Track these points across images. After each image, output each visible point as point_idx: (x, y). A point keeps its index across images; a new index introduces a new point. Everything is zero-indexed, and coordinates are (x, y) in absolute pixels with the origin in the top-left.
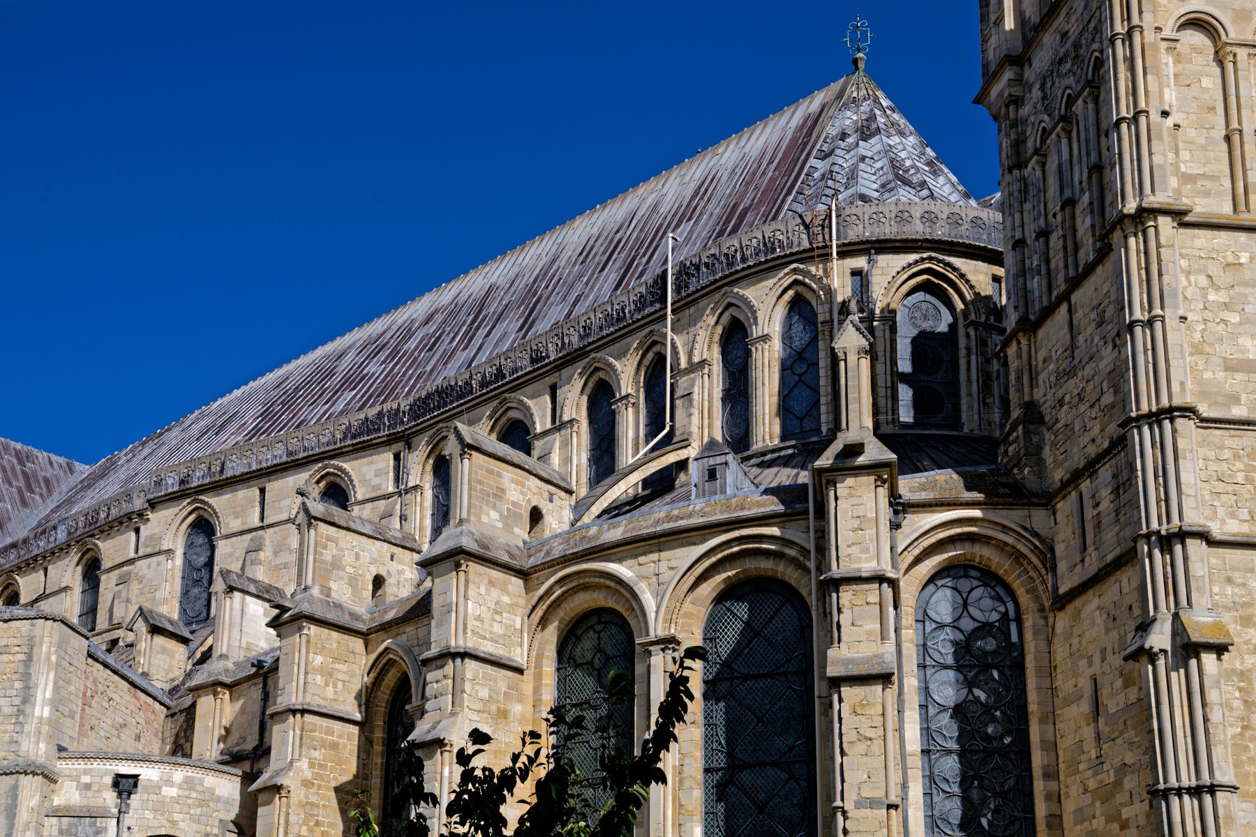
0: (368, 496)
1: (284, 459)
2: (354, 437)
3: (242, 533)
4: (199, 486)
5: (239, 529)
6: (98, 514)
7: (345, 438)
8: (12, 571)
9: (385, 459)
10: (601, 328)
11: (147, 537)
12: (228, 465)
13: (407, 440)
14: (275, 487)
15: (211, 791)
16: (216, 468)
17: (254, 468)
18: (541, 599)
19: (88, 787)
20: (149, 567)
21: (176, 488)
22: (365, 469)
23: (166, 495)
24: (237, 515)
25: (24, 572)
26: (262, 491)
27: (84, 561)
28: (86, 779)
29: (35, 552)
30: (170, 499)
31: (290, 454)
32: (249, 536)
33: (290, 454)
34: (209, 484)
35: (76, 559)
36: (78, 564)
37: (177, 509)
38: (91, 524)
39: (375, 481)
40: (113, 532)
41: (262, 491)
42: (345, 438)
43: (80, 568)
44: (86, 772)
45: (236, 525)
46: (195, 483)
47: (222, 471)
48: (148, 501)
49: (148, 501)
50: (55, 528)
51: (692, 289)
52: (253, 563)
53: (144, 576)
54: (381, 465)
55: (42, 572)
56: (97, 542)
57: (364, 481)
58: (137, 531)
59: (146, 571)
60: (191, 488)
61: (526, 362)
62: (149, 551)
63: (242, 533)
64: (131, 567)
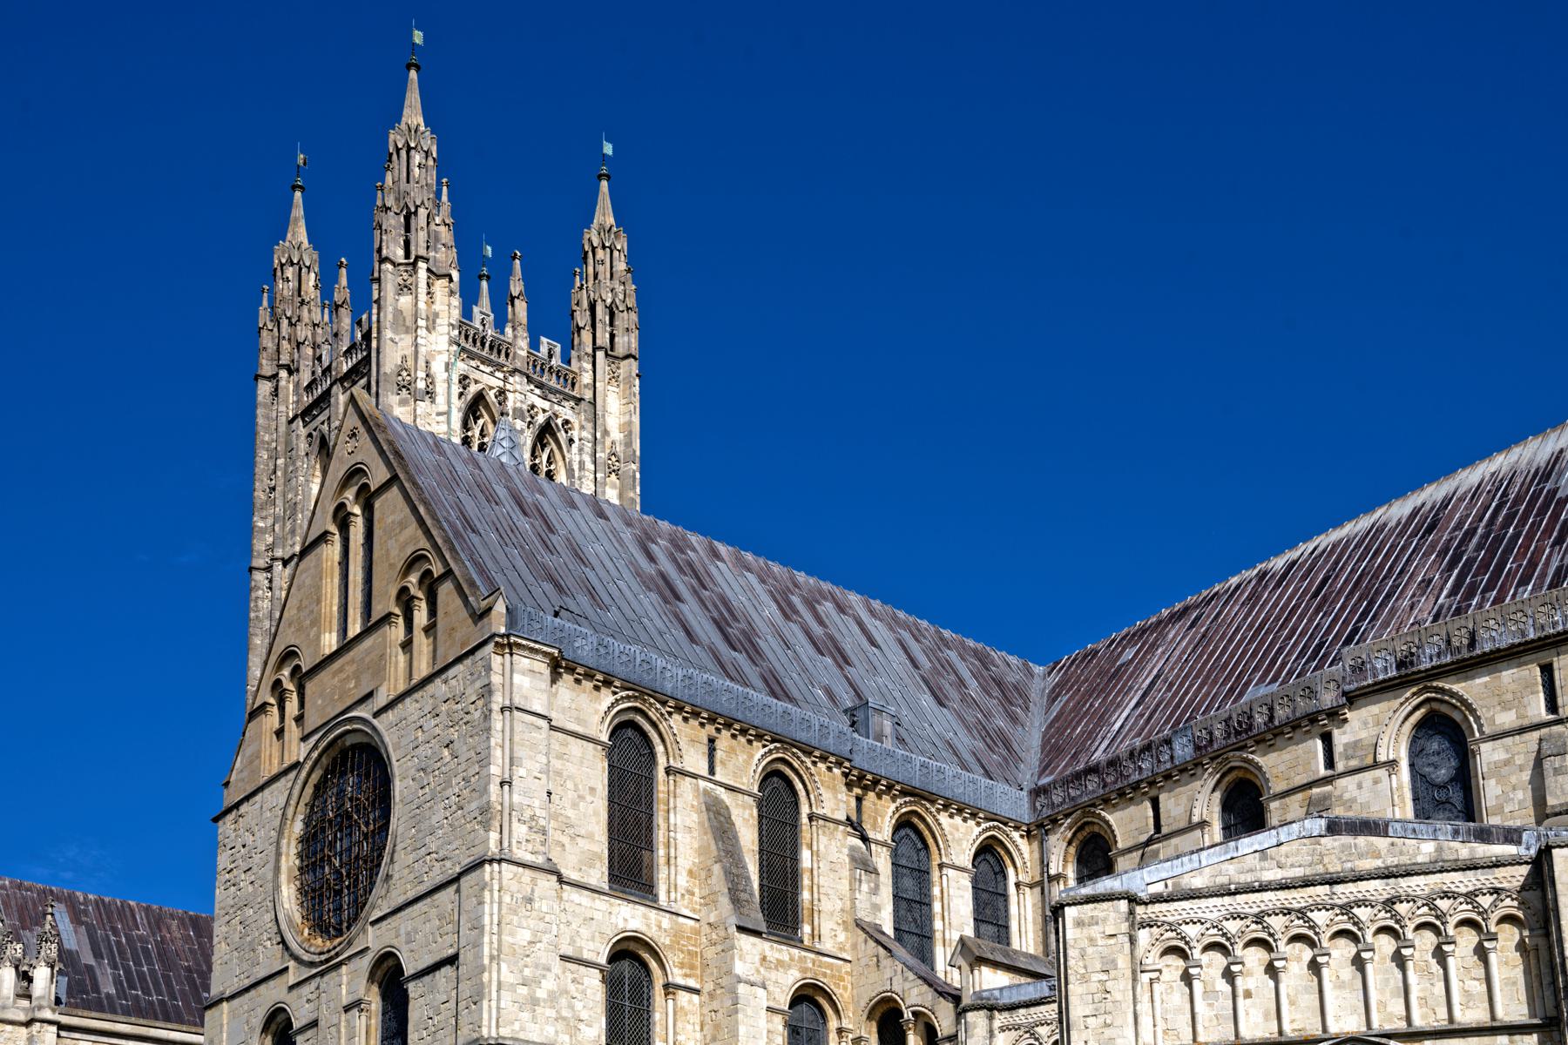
3: (1522, 730)
4: (1433, 668)
5: (1517, 724)
6: (1250, 717)
8: (1094, 805)
11: (1346, 745)
20: (1360, 786)
21: (1393, 673)
23: (1375, 684)
24: (1505, 707)
25: (1114, 806)
26: (1547, 670)
27: (1223, 785)
29: (1136, 777)
30: (1374, 691)
32: (1536, 735)
34: (1452, 663)
35: (1212, 783)
36: (1214, 790)
37: (1396, 703)
38: (1238, 733)
40: (1279, 741)
41: (1547, 670)
43: (1218, 795)
46: (1426, 665)
48: (1344, 694)
49: (1344, 694)
50: (1168, 742)
53: (1354, 800)
55: (1148, 804)
56: (1251, 756)
58: (1327, 739)
59: (1356, 793)
60: (1420, 672)
62: (1354, 763)
63: (1522, 730)
64: (1329, 788)
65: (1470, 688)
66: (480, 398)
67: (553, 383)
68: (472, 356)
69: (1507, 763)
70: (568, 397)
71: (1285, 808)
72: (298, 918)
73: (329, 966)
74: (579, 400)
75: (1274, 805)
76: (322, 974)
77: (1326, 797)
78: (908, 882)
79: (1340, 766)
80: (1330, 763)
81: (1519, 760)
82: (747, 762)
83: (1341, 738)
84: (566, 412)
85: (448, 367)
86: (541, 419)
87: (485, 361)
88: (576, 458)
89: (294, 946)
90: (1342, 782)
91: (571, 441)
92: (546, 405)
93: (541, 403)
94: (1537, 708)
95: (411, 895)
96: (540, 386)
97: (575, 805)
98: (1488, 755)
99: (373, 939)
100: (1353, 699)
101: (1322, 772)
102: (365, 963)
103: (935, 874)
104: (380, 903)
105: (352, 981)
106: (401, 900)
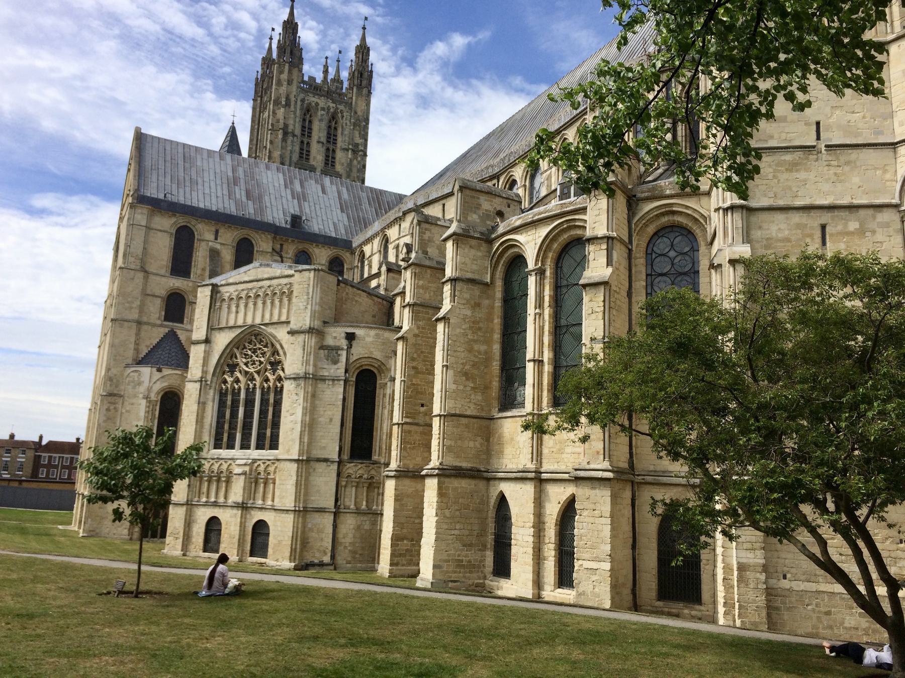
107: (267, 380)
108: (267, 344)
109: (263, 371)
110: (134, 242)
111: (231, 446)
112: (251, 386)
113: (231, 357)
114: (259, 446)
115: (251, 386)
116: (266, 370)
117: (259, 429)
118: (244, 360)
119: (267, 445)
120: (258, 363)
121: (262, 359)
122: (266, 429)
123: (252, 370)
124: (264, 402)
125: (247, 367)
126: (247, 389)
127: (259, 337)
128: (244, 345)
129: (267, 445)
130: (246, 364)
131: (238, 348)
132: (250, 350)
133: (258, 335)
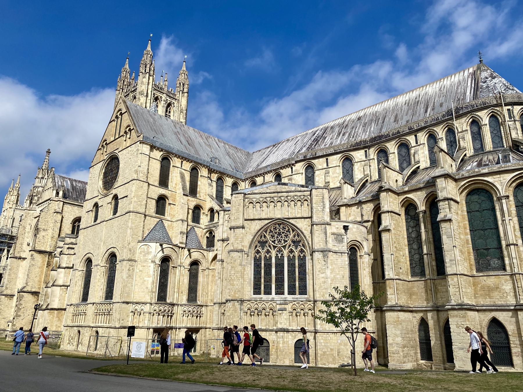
0: (358, 161)
1: (333, 152)
2: (353, 147)
3: (322, 169)
5: (322, 168)
7: (351, 147)
9: (362, 152)
10: (431, 122)
12: (317, 153)
13: (369, 147)
14: (330, 158)
15: (361, 230)
16: (314, 154)
17: (325, 154)
18: (462, 186)
19: (338, 228)
22: (357, 154)
24: (320, 165)
26: (327, 159)
28: (337, 226)
31: (335, 151)
32: (325, 170)
33: (335, 151)
39: (360, 157)
41: (327, 159)
42: (351, 147)
44: (337, 225)
45: (320, 167)
47: (315, 155)
51: (461, 113)
52: (327, 176)
54: (362, 153)
57: (357, 157)
58: (292, 168)
61: (407, 129)
62: (296, 173)
63: (322, 169)
65: (315, 161)
66: (157, 97)
67: (172, 96)
68: (156, 90)
69: (320, 174)
70: (174, 99)
71: (284, 179)
72: (102, 186)
73: (106, 196)
74: (176, 99)
75: (283, 179)
76: (104, 197)
77: (292, 178)
78: (219, 188)
79: (294, 173)
80: (292, 172)
81: (322, 174)
82: (189, 166)
83: (294, 168)
84: (173, 101)
85: (151, 92)
86: (169, 102)
87: (159, 91)
88: (175, 109)
89: (100, 192)
90: (293, 176)
91: (174, 106)
92: (170, 100)
93: (169, 99)
94: (325, 166)
95: (121, 185)
96: (169, 96)
97: (153, 171)
98: (317, 173)
99: (114, 192)
100: (297, 162)
101: (291, 174)
102: (112, 196)
103: (224, 187)
104: (116, 185)
105: (109, 199)
106: (119, 185)
107: (291, 251)
108: (289, 229)
109: (287, 246)
110: (143, 165)
111: (268, 292)
112: (279, 255)
113: (261, 237)
114: (292, 292)
115: (279, 255)
116: (290, 246)
117: (288, 282)
118: (272, 240)
119: (297, 292)
120: (283, 242)
121: (287, 239)
122: (295, 281)
123: (280, 246)
124: (291, 265)
125: (275, 243)
126: (277, 257)
127: (282, 226)
128: (271, 230)
129: (297, 292)
130: (274, 242)
131: (266, 232)
132: (276, 233)
133: (281, 224)
